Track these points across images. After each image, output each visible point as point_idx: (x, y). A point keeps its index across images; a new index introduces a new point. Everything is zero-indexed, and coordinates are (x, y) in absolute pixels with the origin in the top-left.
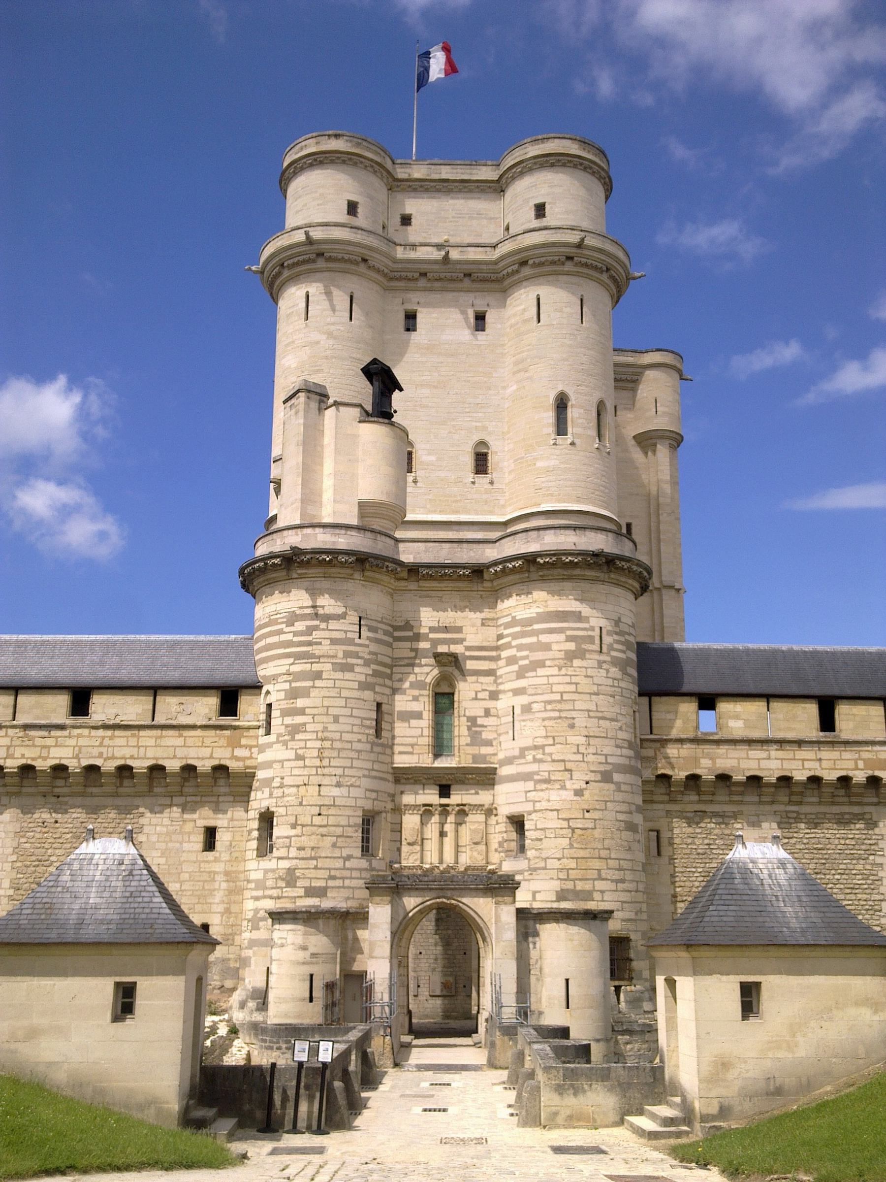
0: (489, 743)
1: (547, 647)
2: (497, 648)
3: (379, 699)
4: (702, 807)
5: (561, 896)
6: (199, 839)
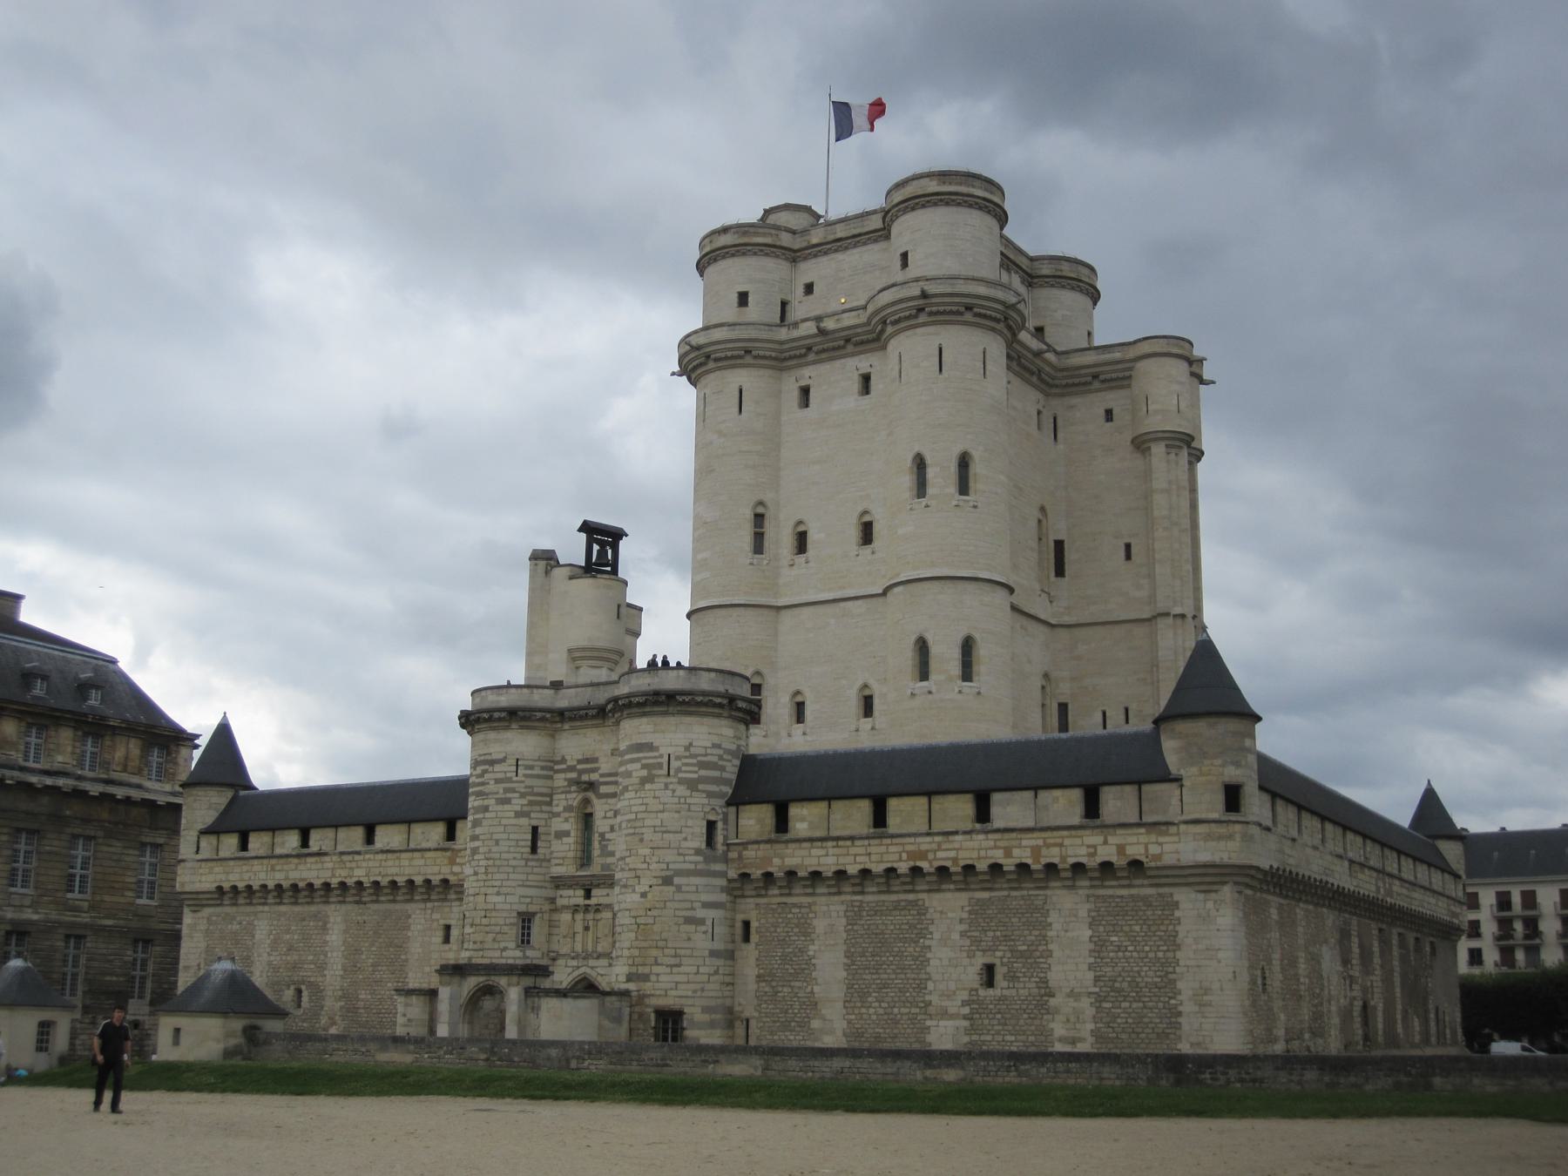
0: (612, 854)
1: (629, 774)
2: (615, 774)
3: (535, 823)
4: (784, 899)
5: (630, 978)
6: (438, 937)
